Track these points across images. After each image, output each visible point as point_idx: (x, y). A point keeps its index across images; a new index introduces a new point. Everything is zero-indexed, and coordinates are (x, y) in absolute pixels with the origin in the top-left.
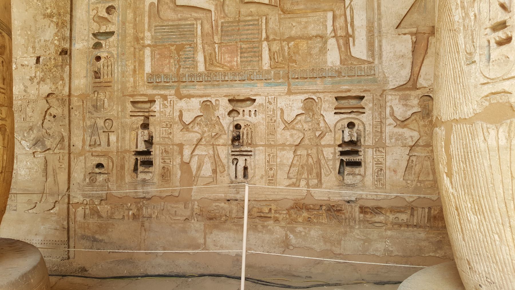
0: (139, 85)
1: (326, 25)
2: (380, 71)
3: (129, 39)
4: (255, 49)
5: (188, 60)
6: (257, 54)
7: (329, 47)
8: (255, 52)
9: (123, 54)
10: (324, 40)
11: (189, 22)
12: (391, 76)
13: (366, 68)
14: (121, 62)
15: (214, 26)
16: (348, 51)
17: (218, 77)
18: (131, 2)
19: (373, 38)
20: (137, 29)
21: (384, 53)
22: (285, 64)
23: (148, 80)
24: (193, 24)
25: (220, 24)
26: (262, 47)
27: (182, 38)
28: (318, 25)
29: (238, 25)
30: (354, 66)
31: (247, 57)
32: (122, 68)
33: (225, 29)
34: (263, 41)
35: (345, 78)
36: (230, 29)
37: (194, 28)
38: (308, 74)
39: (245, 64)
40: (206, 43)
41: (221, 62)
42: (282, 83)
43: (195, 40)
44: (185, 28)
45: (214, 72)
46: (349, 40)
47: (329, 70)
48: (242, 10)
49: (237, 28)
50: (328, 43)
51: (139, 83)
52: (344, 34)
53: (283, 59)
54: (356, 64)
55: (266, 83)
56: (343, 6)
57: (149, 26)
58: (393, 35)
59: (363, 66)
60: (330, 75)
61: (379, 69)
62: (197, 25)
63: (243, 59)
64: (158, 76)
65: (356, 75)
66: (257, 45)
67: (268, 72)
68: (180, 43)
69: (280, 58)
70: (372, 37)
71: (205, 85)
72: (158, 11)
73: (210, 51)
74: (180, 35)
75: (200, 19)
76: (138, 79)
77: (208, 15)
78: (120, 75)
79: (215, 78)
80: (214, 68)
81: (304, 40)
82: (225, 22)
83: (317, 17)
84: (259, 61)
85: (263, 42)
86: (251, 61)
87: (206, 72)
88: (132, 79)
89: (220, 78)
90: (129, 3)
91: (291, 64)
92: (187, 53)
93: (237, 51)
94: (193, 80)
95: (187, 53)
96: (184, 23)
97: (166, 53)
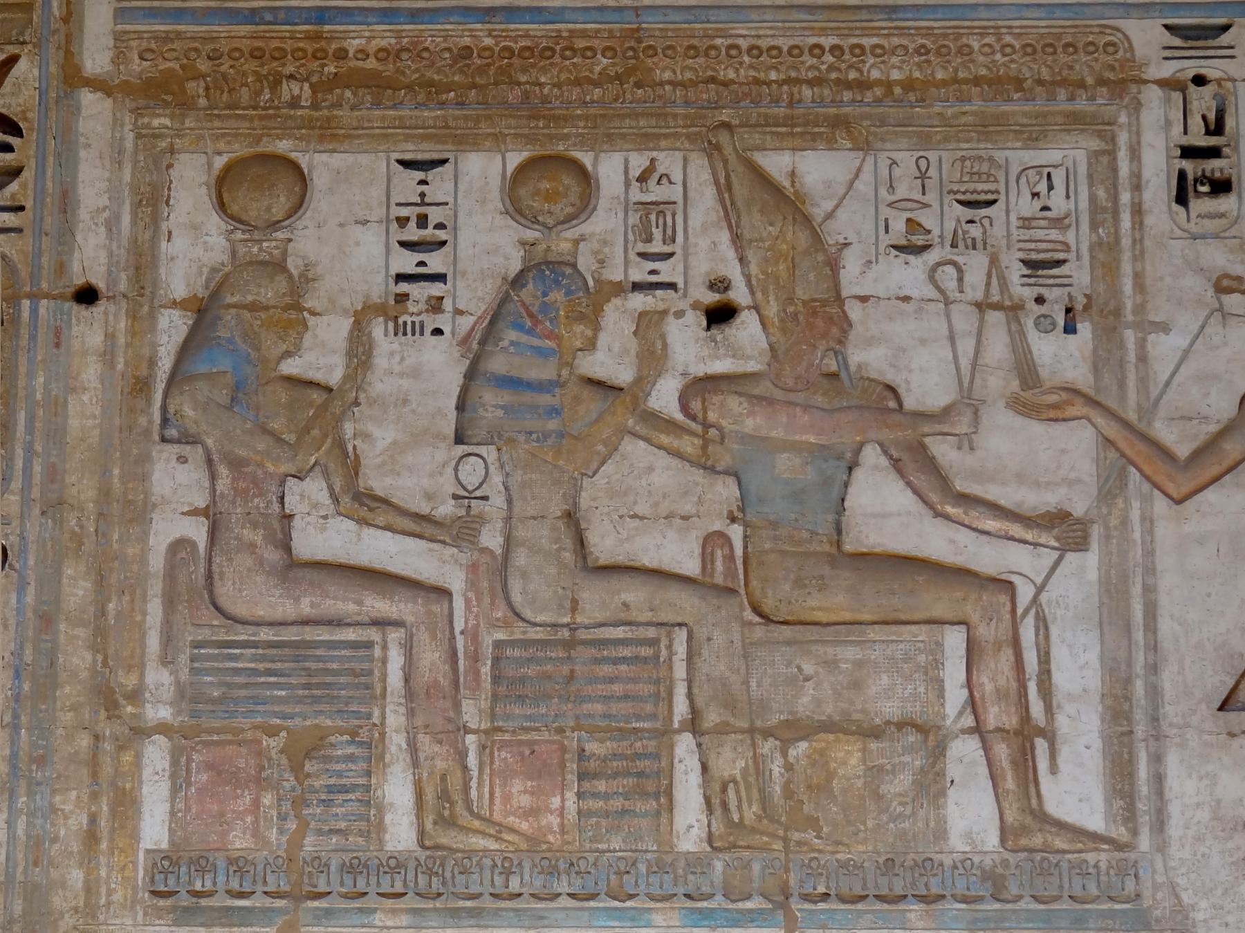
0: (109, 904)
1: (941, 682)
2: (1160, 879)
3: (68, 692)
4: (642, 764)
5: (341, 797)
6: (651, 787)
7: (953, 770)
8: (640, 774)
9: (41, 761)
10: (931, 743)
11: (350, 635)
12: (1204, 904)
13: (1103, 865)
14: (31, 794)
15: (461, 655)
16: (1032, 790)
17: (475, 877)
18: (82, 527)
19: (1131, 745)
20: (111, 651)
21: (1174, 809)
22: (774, 836)
23: (152, 881)
24: (369, 645)
25: (488, 651)
26: (671, 756)
27: (316, 700)
28: (908, 678)
29: (569, 658)
30: (1053, 858)
31: (606, 797)
32: (29, 824)
33: (511, 673)
34: (679, 731)
35: (1022, 904)
36: (532, 671)
37: (371, 659)
38: (870, 878)
39: (598, 823)
40: (427, 726)
41: (491, 814)
42: (761, 911)
43: (377, 713)
44: (332, 659)
45: (459, 855)
46: (1033, 748)
47: (955, 867)
48: (585, 595)
49: (566, 670)
50: (949, 754)
51: (110, 892)
52: (1011, 721)
53: (764, 809)
54: (1065, 846)
55: (693, 910)
56: (1008, 607)
57: (168, 639)
58: (1206, 737)
59: (1091, 857)
60: (961, 885)
61: (1154, 872)
62: (385, 647)
63: (585, 805)
64: (202, 864)
65: (1066, 894)
66: (651, 745)
67: (696, 863)
68: (308, 723)
69: (750, 807)
70: (1126, 739)
71: (415, 912)
72: (209, 576)
73: (440, 765)
74: (307, 686)
75: (398, 624)
76: (109, 877)
77: (436, 608)
78: (20, 856)
79: (460, 879)
80: (461, 837)
81: (852, 738)
82: (512, 643)
83: (901, 646)
84: (658, 813)
85: (677, 737)
86: (624, 812)
87: (422, 855)
88: (76, 877)
89: (487, 882)
90: (73, 532)
91: (796, 836)
92: (338, 767)
93: (562, 764)
94: (361, 885)
95: (338, 767)
96: (326, 637)
97: (241, 763)
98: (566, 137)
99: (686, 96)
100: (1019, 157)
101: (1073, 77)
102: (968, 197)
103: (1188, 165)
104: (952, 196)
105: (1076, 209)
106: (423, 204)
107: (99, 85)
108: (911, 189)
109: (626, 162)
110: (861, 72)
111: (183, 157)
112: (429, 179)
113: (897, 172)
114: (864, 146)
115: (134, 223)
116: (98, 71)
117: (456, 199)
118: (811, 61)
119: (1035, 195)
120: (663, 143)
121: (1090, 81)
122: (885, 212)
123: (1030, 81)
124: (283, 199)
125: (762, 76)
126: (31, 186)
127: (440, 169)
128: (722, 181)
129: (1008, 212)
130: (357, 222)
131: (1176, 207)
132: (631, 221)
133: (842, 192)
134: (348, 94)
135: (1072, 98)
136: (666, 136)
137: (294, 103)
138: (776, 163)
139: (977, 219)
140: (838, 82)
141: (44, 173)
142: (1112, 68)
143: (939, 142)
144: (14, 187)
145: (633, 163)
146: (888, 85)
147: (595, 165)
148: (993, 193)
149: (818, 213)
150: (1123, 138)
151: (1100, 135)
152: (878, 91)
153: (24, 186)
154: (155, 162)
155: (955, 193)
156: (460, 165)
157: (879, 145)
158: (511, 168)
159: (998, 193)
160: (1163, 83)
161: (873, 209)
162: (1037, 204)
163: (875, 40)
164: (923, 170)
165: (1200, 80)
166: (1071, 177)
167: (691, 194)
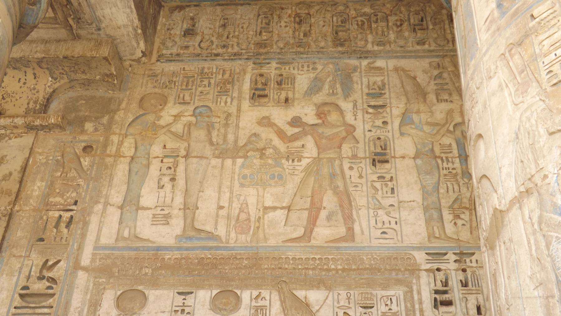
98: (232, 286)
99: (272, 273)
100: (380, 293)
101: (397, 268)
102: (364, 305)
103: (437, 296)
104: (359, 305)
105: (401, 310)
106: (184, 306)
107: (85, 269)
108: (345, 303)
109: (251, 293)
110: (328, 267)
111: (108, 291)
112: (186, 298)
113: (340, 297)
114: (329, 288)
115: (88, 312)
116: (85, 265)
117: (194, 305)
118: (311, 262)
119: (387, 305)
120: (263, 287)
121: (402, 269)
122: (336, 310)
123: (383, 269)
124: (138, 305)
125: (296, 267)
126: (56, 300)
127: (190, 295)
128: (283, 300)
129: (377, 310)
130: (161, 312)
131: (434, 310)
132: (252, 312)
133: (322, 303)
134: (163, 272)
135: (397, 275)
136: (265, 286)
137: (146, 274)
138: (300, 294)
139: (367, 313)
140: (320, 269)
141: (62, 296)
142: (410, 266)
143: (354, 288)
144: (51, 300)
145: (253, 294)
146: (337, 270)
147: (241, 294)
148: (372, 304)
149: (314, 310)
150: (415, 288)
151: (407, 286)
152: (334, 272)
153: (54, 300)
154: (98, 293)
155: (360, 304)
156: (197, 294)
157: (334, 288)
158: (213, 296)
159: (374, 304)
160: (426, 270)
161: (332, 309)
162: (387, 308)
163: (333, 257)
164: (349, 296)
165: (438, 270)
166: (398, 300)
167: (272, 303)
